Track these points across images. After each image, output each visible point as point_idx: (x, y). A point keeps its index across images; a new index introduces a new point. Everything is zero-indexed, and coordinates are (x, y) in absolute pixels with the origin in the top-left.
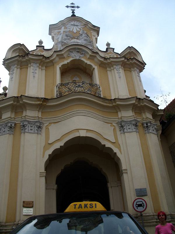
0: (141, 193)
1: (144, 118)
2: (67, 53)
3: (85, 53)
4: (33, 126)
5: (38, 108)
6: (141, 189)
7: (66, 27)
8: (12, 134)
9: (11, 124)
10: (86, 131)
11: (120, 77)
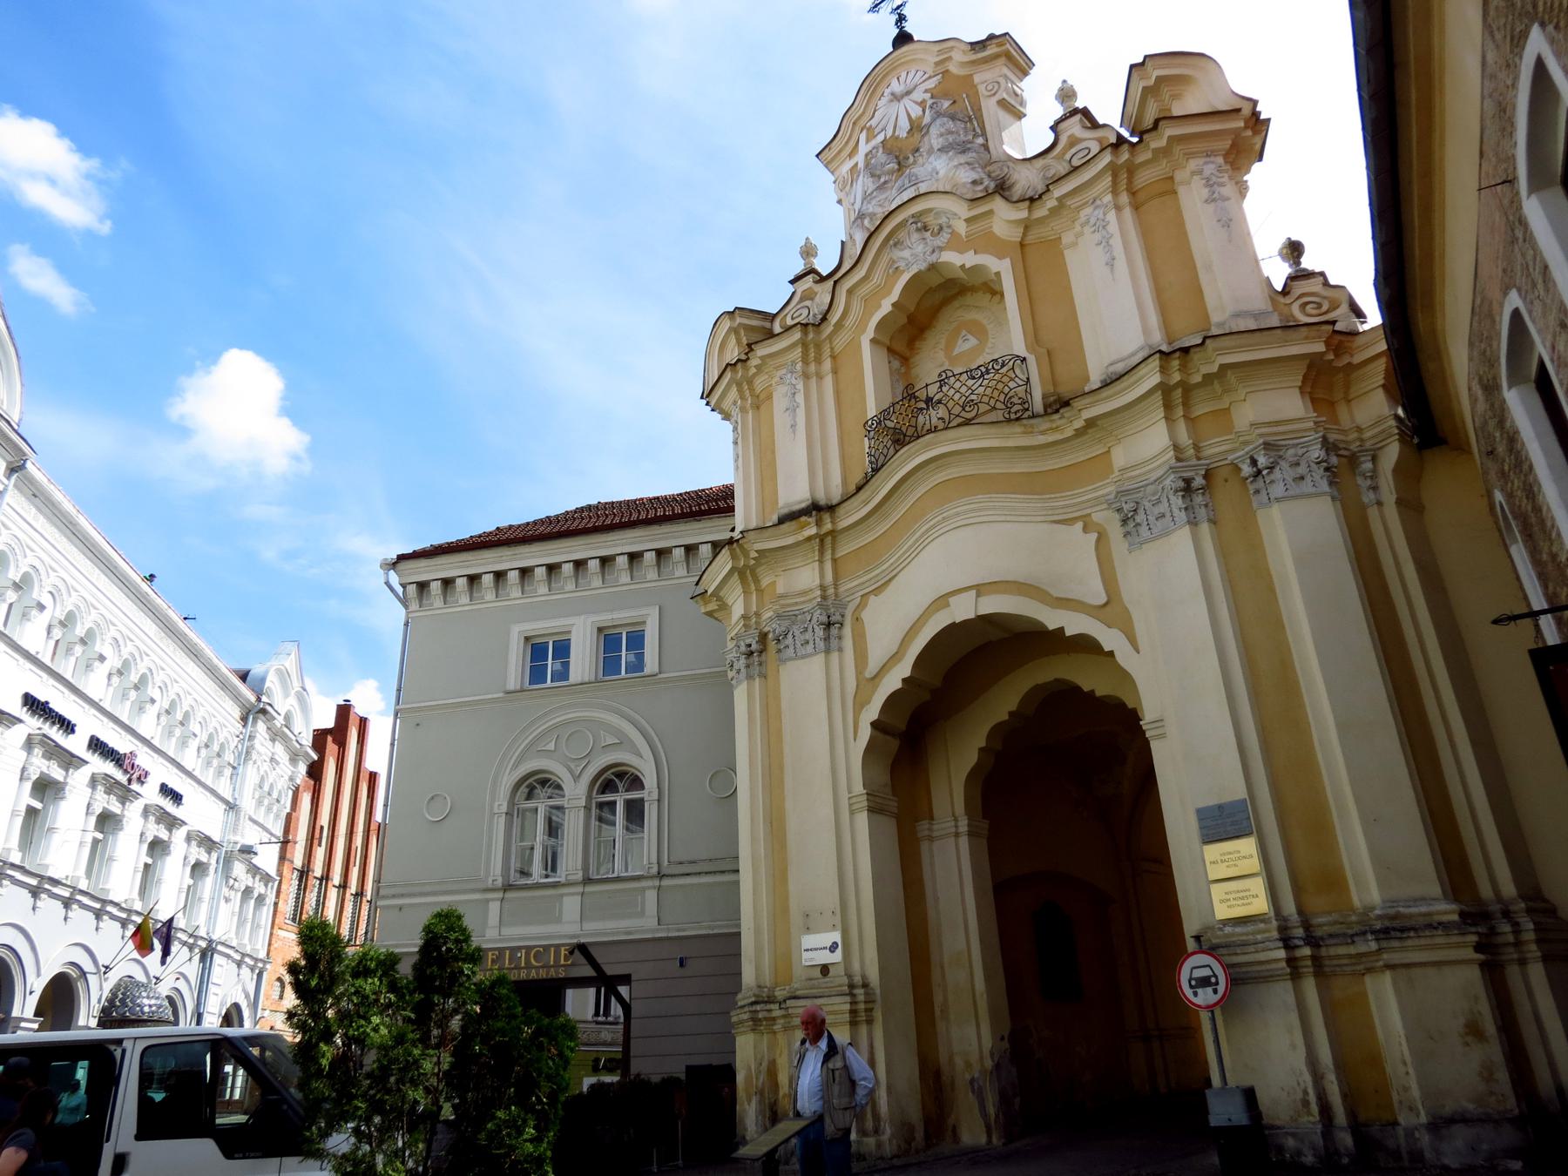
1: (1239, 435)
2: (884, 259)
3: (952, 222)
4: (810, 629)
5: (817, 553)
6: (1220, 807)
9: (748, 642)
10: (973, 592)
11: (1111, 263)
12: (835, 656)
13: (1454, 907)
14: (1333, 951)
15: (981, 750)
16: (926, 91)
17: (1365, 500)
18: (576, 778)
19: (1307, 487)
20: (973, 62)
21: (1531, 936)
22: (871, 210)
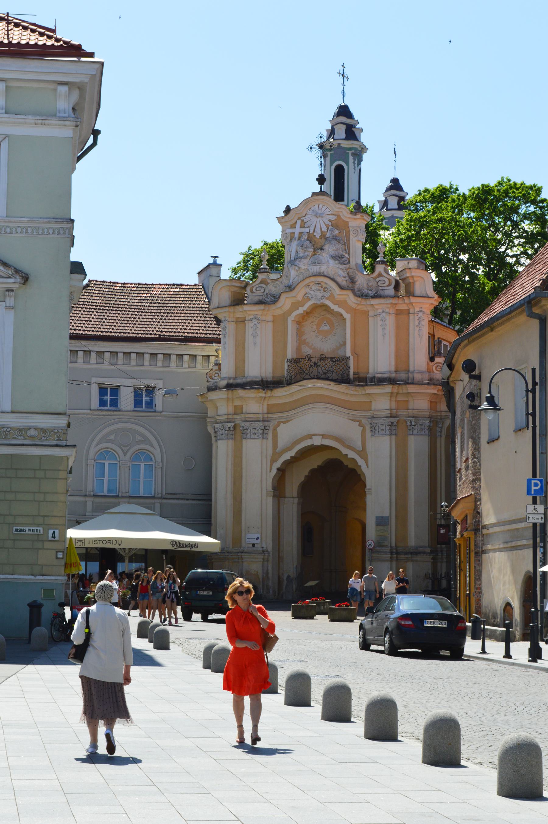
0: (381, 521)
4: (257, 429)
6: (382, 517)
7: (303, 220)
8: (232, 439)
9: (229, 426)
10: (321, 436)
12: (265, 440)
13: (430, 549)
14: (401, 556)
15: (306, 476)
16: (330, 221)
17: (438, 435)
18: (125, 454)
19: (423, 433)
20: (349, 218)
21: (445, 557)
22: (300, 266)
